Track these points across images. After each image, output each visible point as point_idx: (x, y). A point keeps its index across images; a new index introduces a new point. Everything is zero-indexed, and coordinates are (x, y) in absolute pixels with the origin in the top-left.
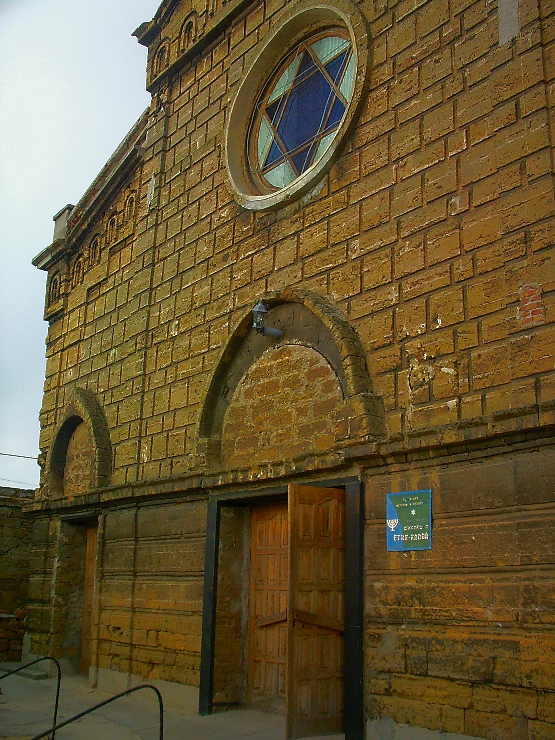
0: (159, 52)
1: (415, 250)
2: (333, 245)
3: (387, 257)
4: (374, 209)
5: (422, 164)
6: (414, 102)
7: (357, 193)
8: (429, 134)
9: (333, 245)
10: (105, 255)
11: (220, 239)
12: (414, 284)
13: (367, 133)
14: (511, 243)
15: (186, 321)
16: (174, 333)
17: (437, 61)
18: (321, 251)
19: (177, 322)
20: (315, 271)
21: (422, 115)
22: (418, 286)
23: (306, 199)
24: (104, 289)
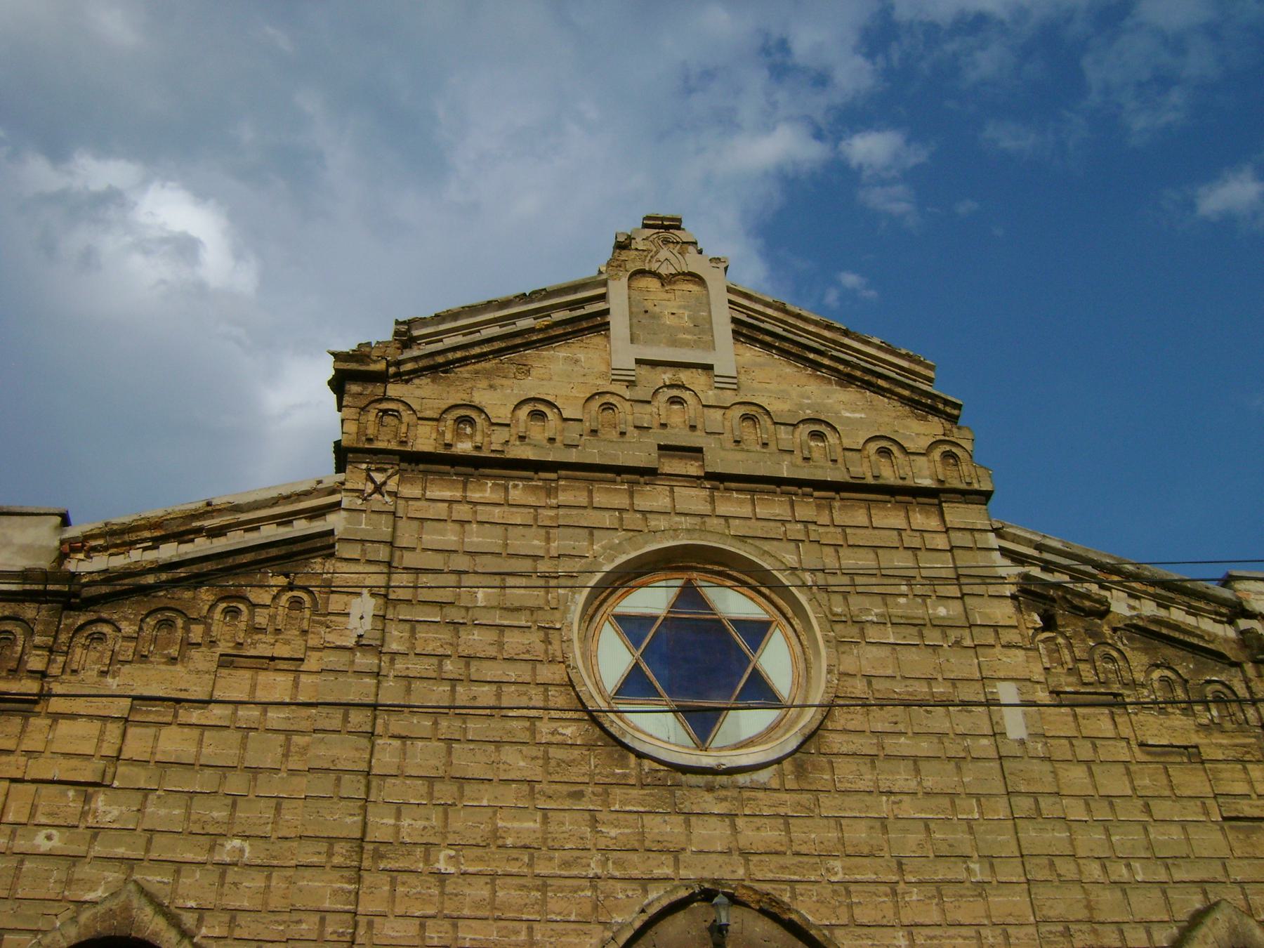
0: (380, 411)
1: (928, 901)
2: (798, 854)
3: (886, 895)
4: (859, 834)
5: (922, 811)
6: (902, 740)
7: (829, 805)
8: (930, 784)
9: (798, 854)
10: (202, 660)
11: (559, 765)
12: (931, 938)
13: (836, 742)
14: (1051, 932)
15: (480, 859)
16: (442, 866)
17: (927, 712)
18: (777, 853)
19: (453, 853)
20: (770, 876)
21: (915, 759)
22: (935, 942)
23: (742, 779)
24: (195, 716)
